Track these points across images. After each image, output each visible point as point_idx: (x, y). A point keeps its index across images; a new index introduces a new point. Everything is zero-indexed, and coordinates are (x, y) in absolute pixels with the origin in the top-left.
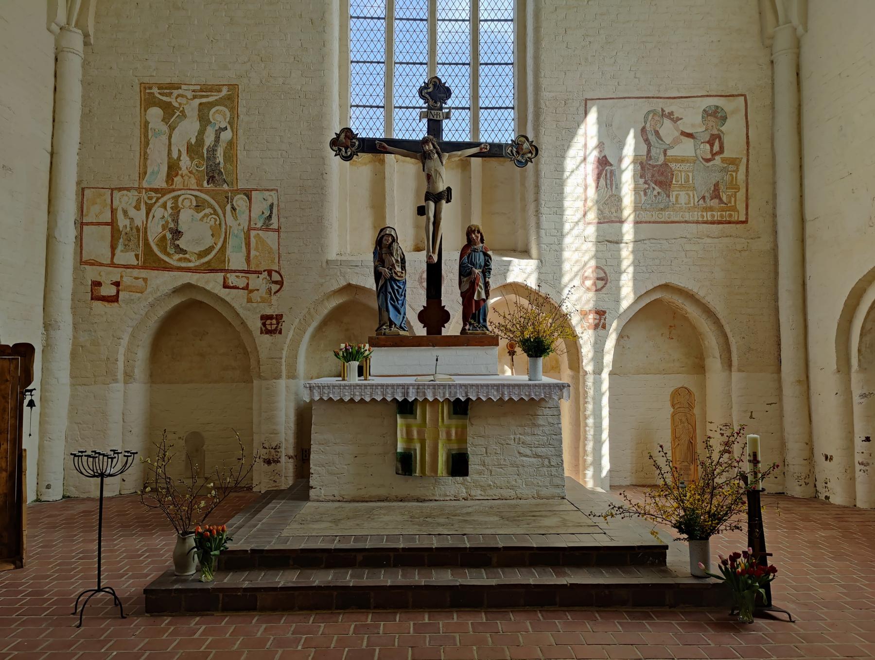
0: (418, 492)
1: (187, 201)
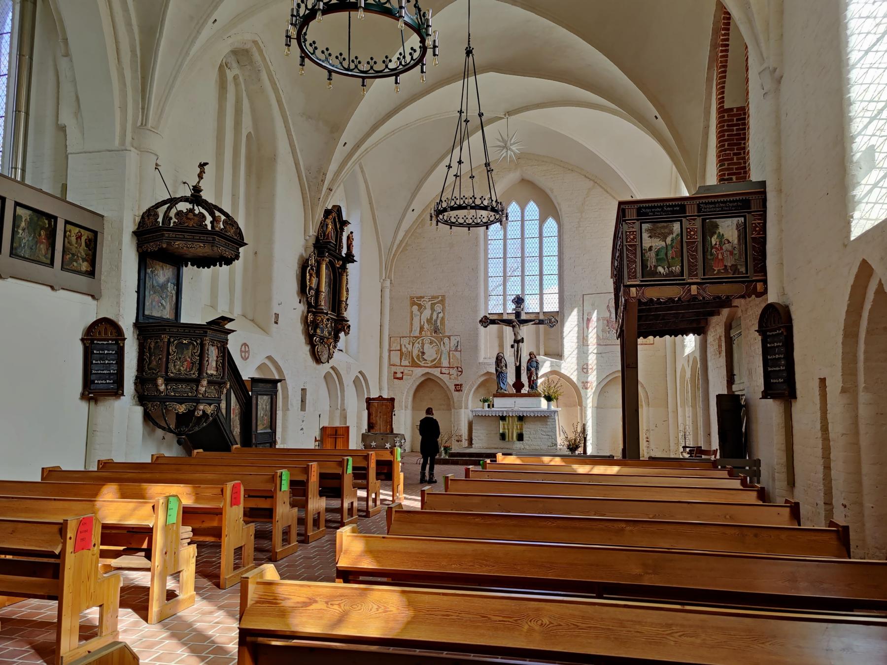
1: (427, 341)
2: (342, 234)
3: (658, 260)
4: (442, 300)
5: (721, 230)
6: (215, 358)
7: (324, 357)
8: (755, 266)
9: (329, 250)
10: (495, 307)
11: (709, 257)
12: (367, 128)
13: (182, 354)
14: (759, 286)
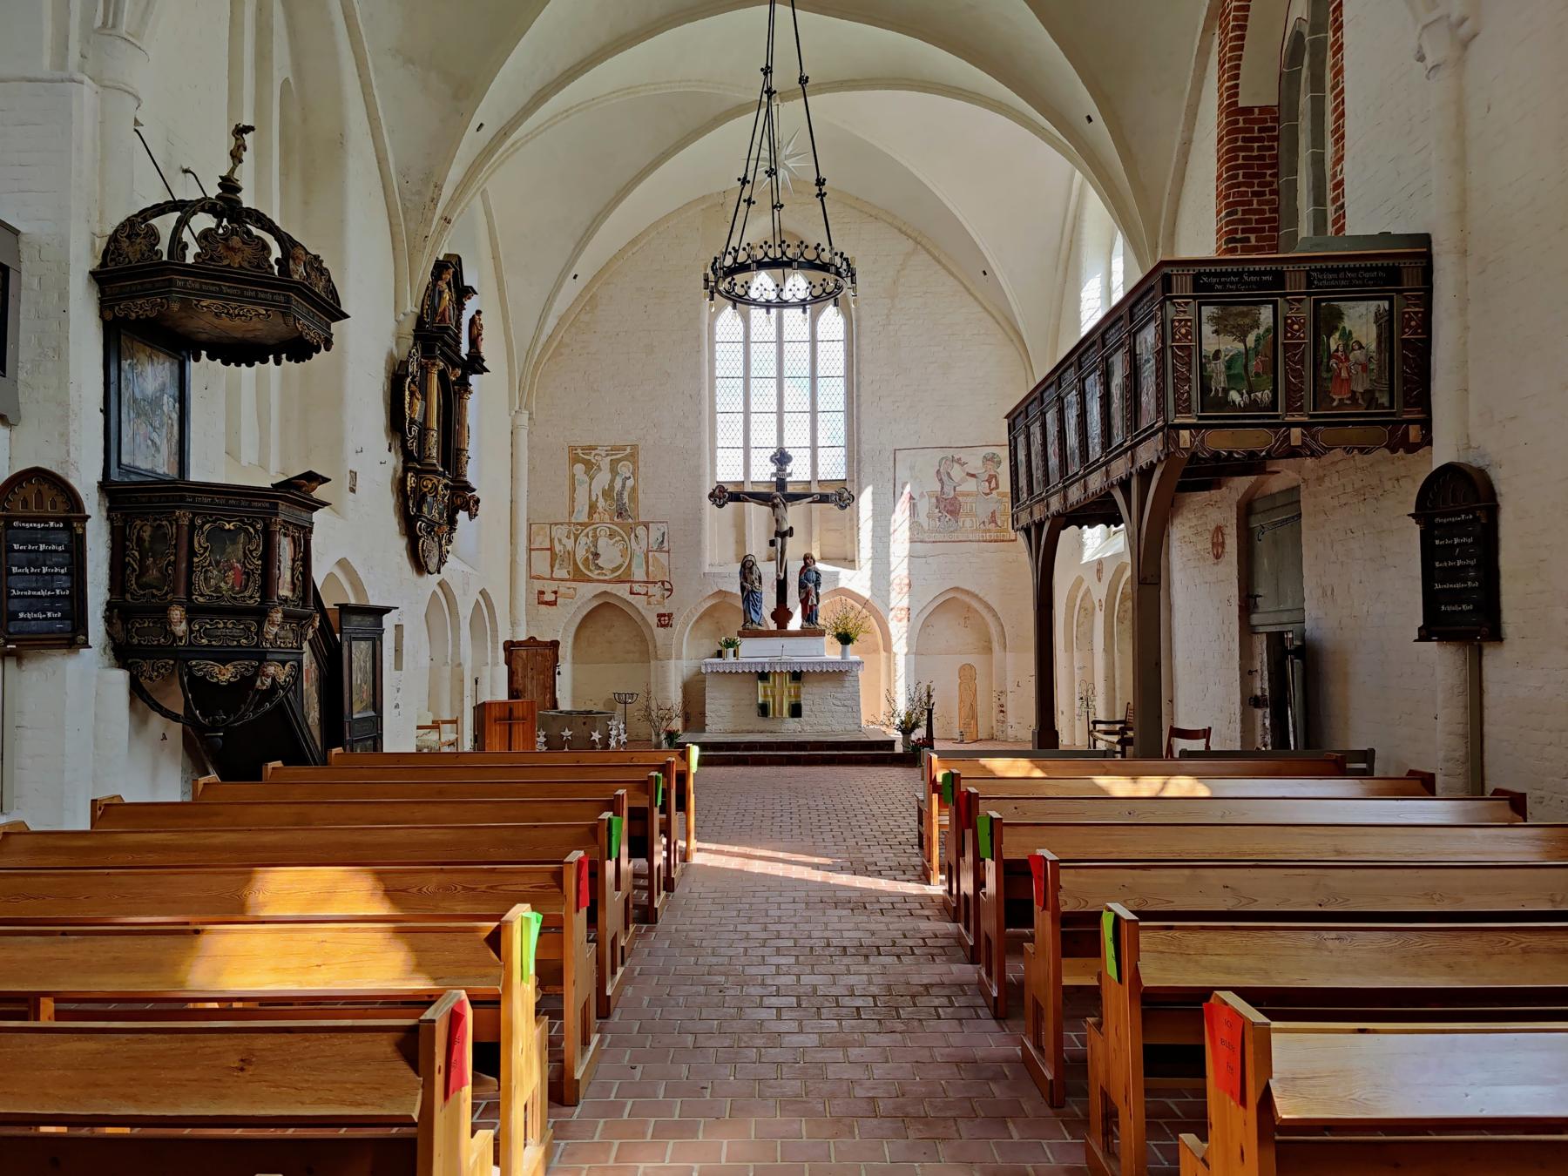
0: (772, 728)
1: (603, 531)
2: (459, 316)
3: (1229, 377)
4: (632, 455)
5: (1347, 324)
6: (290, 563)
7: (432, 563)
8: (1405, 394)
9: (446, 344)
10: (728, 470)
11: (1325, 375)
12: (524, 98)
13: (223, 551)
14: (1414, 433)
